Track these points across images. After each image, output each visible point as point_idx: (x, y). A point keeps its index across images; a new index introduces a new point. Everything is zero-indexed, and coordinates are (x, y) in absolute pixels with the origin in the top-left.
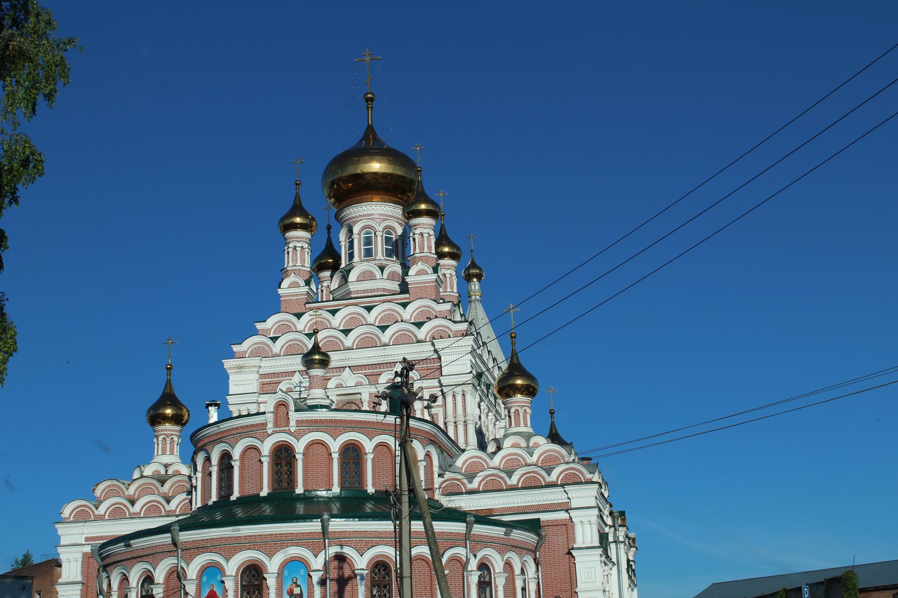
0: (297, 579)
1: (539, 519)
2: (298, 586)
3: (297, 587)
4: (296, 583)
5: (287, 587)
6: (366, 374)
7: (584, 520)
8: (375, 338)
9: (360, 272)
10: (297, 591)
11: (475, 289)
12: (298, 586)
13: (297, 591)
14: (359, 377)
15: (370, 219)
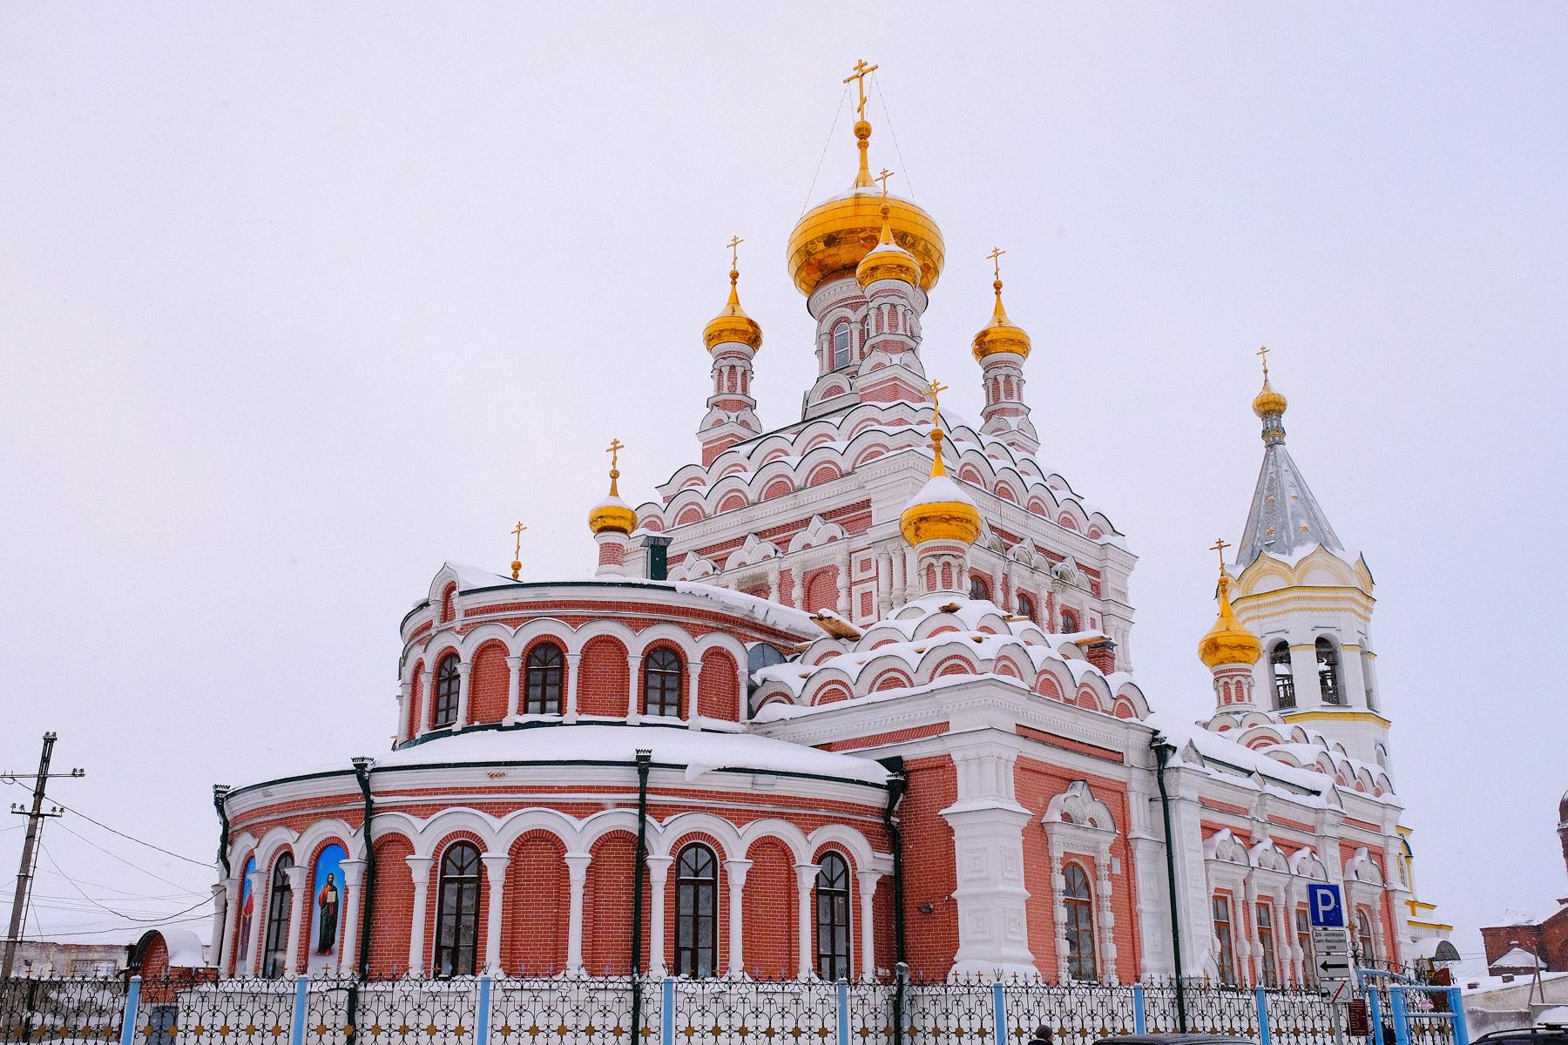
0: (333, 878)
1: (900, 757)
2: (334, 889)
3: (331, 891)
4: (330, 883)
5: (318, 894)
6: (777, 541)
7: (971, 754)
8: (788, 482)
9: (825, 391)
10: (331, 898)
11: (1273, 426)
12: (334, 889)
13: (331, 898)
14: (768, 547)
15: (842, 306)
